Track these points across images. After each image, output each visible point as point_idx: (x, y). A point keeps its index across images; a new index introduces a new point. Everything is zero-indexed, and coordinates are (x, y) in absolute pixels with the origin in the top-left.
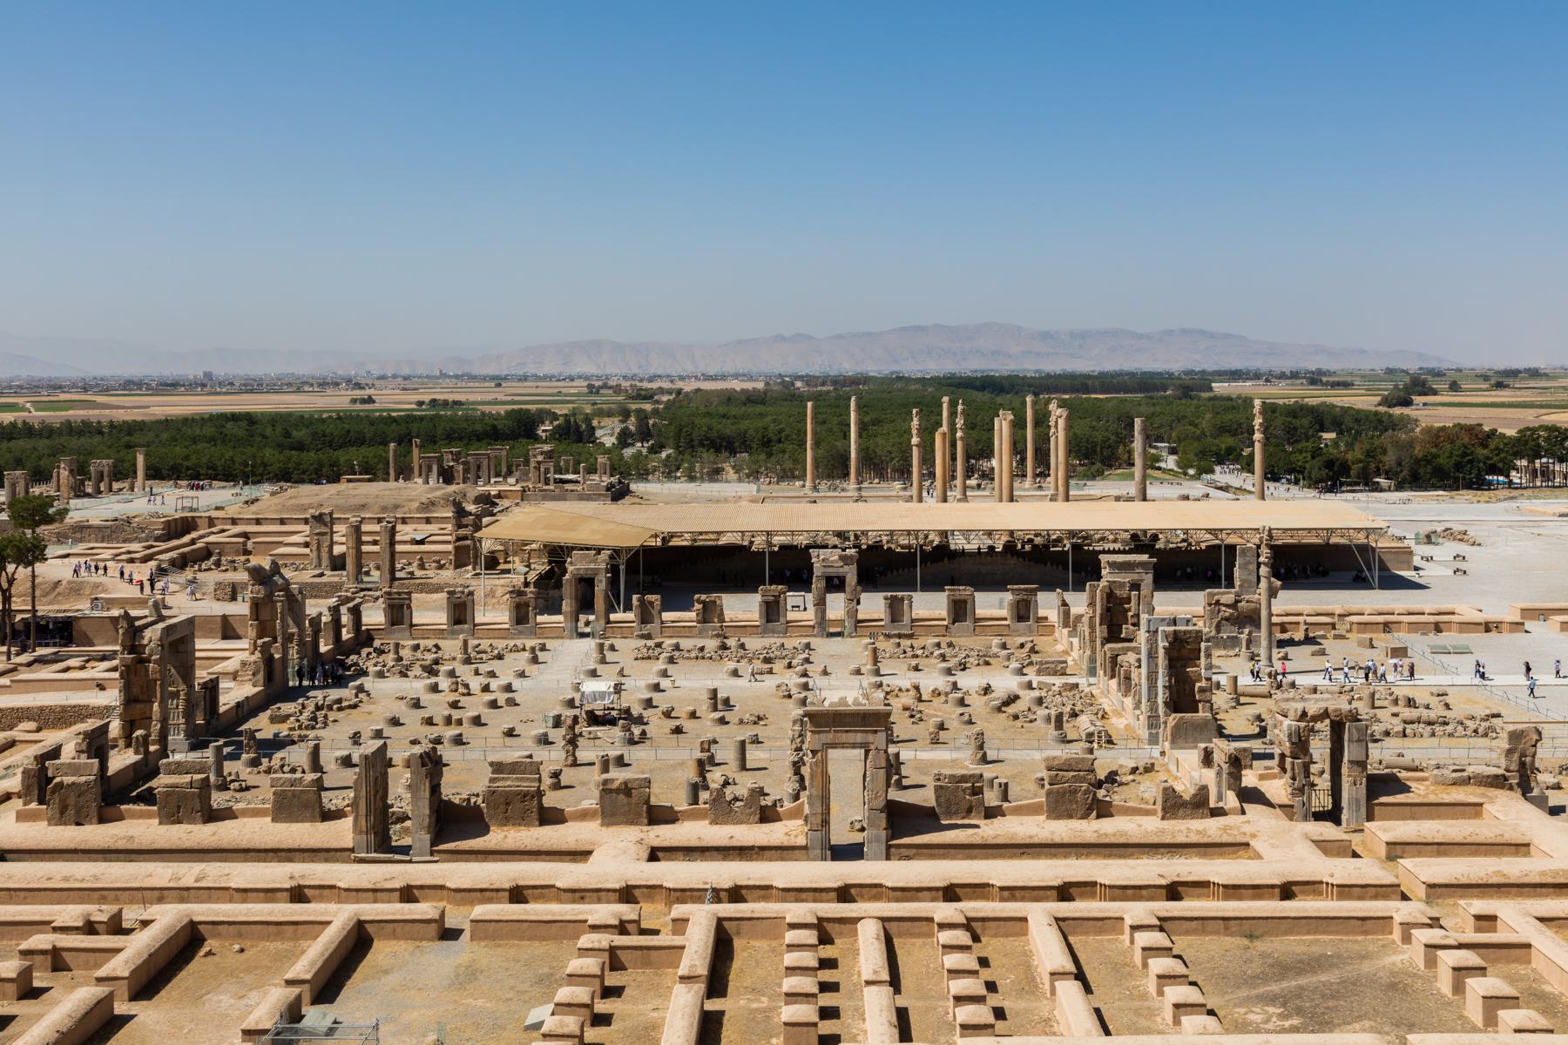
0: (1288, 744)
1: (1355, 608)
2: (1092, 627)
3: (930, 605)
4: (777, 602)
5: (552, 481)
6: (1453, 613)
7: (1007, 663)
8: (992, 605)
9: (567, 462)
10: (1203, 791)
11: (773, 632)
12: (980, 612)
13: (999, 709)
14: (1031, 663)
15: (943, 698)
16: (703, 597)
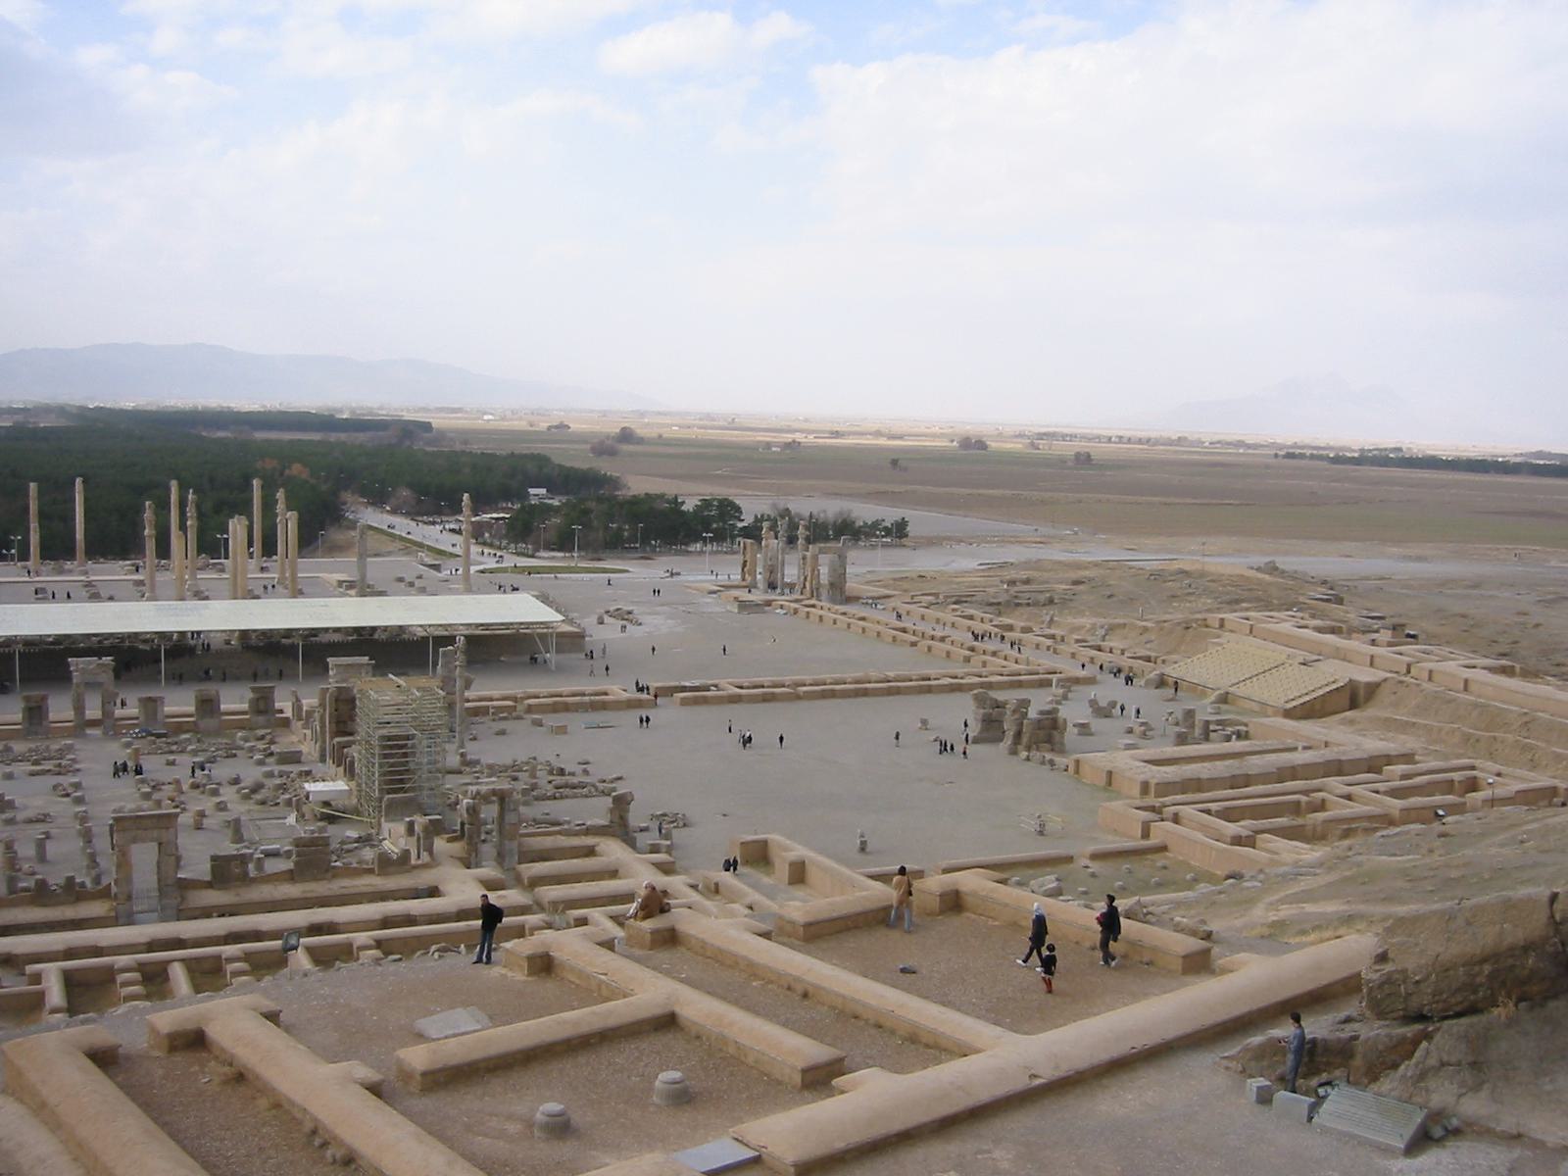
0: (466, 816)
1: (532, 690)
2: (323, 726)
3: (179, 702)
6: (606, 694)
7: (251, 755)
8: (234, 700)
10: (406, 854)
12: (223, 707)
13: (246, 797)
14: (272, 754)
15: (201, 789)
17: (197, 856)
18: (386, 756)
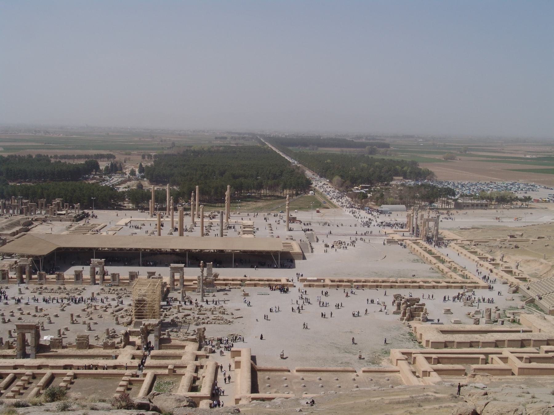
4: (80, 275)
5: (56, 214)
9: (66, 205)
11: (78, 283)
16: (58, 273)
17: (46, 338)
18: (137, 307)
